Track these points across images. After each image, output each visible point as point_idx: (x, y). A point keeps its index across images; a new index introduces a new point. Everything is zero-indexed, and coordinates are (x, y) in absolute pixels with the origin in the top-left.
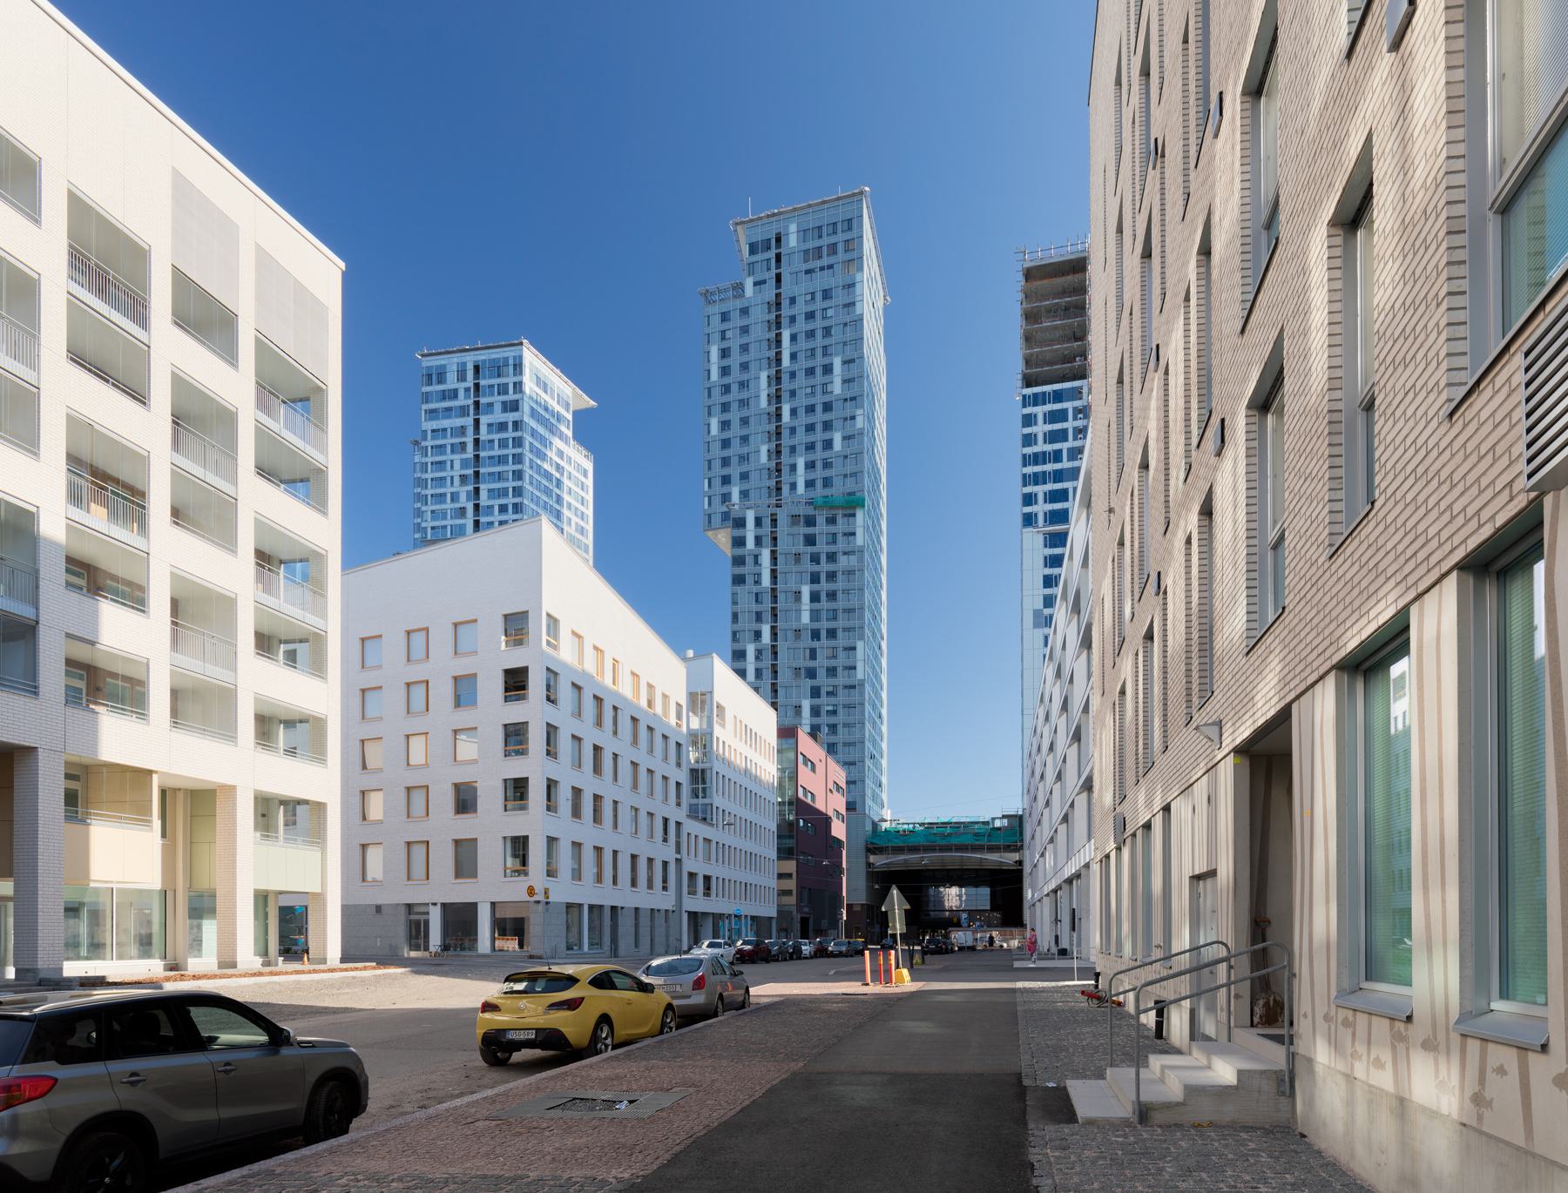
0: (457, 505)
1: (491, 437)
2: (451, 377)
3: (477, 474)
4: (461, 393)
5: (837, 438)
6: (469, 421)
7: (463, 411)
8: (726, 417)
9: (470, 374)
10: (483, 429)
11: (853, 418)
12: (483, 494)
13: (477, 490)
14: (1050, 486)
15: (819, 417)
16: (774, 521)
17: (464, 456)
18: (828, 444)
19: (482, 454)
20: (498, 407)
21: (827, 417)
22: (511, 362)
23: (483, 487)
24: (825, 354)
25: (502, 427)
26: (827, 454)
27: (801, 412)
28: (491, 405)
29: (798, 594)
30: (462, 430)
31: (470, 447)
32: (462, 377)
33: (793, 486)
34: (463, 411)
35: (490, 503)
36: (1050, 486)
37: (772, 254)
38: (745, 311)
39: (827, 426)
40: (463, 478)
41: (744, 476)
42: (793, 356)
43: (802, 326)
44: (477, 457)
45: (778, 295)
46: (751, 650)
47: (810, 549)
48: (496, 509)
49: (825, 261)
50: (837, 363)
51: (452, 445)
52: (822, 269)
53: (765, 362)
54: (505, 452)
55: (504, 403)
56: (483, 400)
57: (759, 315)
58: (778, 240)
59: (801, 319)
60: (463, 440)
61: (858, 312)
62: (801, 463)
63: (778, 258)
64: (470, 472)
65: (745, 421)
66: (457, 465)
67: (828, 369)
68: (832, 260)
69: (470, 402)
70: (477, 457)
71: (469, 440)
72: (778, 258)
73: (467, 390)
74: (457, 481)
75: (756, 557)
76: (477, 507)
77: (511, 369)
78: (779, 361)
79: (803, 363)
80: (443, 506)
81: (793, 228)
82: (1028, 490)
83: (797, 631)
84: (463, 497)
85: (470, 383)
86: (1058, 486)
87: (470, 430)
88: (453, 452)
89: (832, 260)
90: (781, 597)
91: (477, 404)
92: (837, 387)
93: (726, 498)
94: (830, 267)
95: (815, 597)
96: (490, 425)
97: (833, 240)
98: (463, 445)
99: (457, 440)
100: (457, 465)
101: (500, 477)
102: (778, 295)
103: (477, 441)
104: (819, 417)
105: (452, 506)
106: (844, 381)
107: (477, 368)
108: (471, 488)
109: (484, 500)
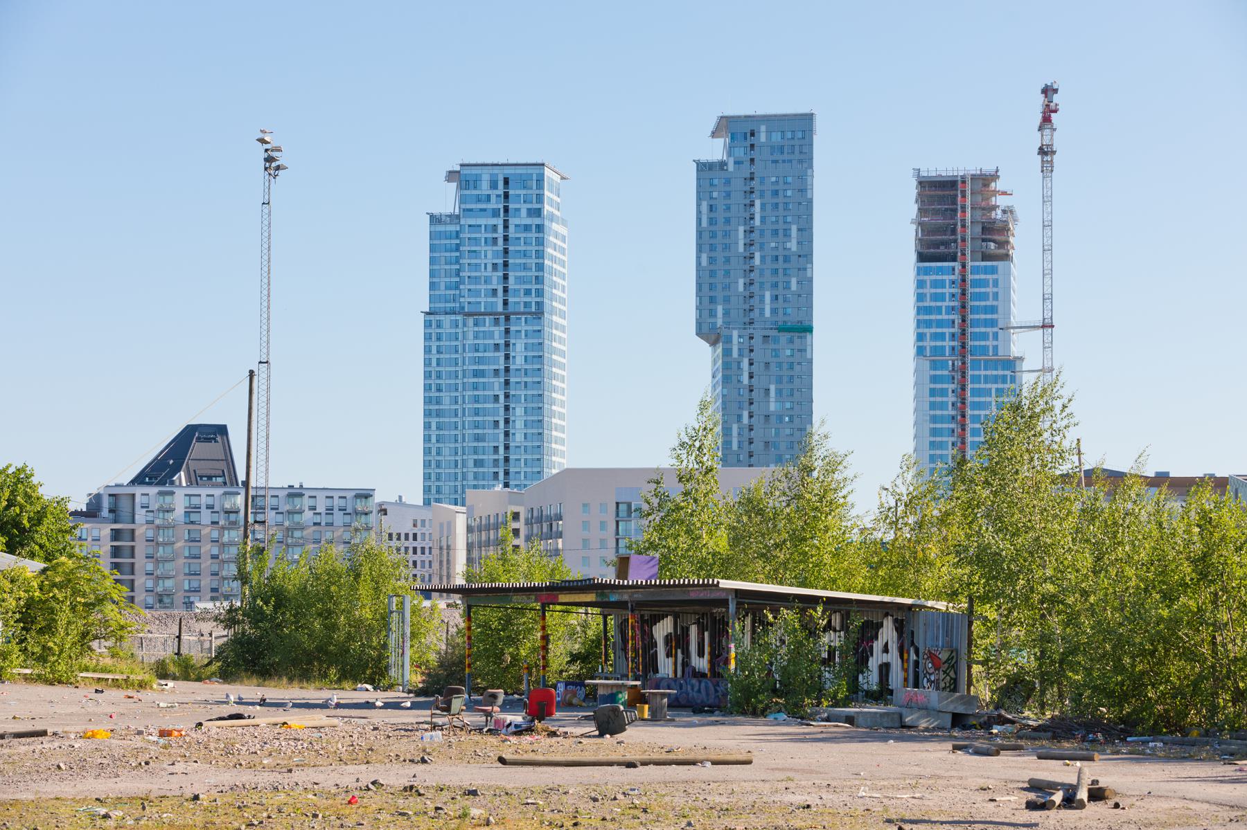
0: (490, 287)
1: (518, 235)
2: (485, 185)
3: (506, 264)
6: (499, 222)
7: (495, 213)
8: (713, 254)
9: (501, 184)
10: (512, 228)
11: (805, 269)
12: (511, 280)
13: (506, 277)
17: (495, 248)
18: (787, 286)
20: (524, 213)
22: (535, 177)
23: (511, 275)
25: (527, 228)
27: (768, 259)
28: (518, 210)
29: (768, 390)
31: (501, 241)
32: (494, 185)
33: (762, 310)
35: (517, 287)
38: (728, 182)
40: (495, 266)
41: (727, 300)
42: (763, 219)
43: (768, 198)
44: (506, 251)
46: (735, 427)
47: (775, 360)
48: (522, 292)
49: (786, 157)
50: (794, 228)
52: (784, 161)
53: (742, 220)
54: (529, 248)
55: (529, 210)
56: (511, 206)
57: (738, 185)
58: (752, 134)
59: (768, 194)
64: (500, 261)
65: (728, 260)
66: (490, 255)
67: (787, 233)
68: (790, 157)
69: (501, 206)
70: (506, 251)
73: (498, 196)
74: (490, 267)
75: (739, 363)
76: (506, 290)
77: (535, 182)
80: (478, 287)
81: (763, 128)
83: (767, 417)
84: (495, 280)
87: (501, 228)
89: (790, 157)
91: (506, 210)
92: (793, 245)
93: (712, 314)
94: (790, 161)
95: (779, 392)
97: (792, 143)
99: (490, 235)
100: (490, 255)
101: (525, 267)
103: (506, 239)
105: (485, 287)
107: (506, 181)
108: (501, 274)
109: (512, 284)
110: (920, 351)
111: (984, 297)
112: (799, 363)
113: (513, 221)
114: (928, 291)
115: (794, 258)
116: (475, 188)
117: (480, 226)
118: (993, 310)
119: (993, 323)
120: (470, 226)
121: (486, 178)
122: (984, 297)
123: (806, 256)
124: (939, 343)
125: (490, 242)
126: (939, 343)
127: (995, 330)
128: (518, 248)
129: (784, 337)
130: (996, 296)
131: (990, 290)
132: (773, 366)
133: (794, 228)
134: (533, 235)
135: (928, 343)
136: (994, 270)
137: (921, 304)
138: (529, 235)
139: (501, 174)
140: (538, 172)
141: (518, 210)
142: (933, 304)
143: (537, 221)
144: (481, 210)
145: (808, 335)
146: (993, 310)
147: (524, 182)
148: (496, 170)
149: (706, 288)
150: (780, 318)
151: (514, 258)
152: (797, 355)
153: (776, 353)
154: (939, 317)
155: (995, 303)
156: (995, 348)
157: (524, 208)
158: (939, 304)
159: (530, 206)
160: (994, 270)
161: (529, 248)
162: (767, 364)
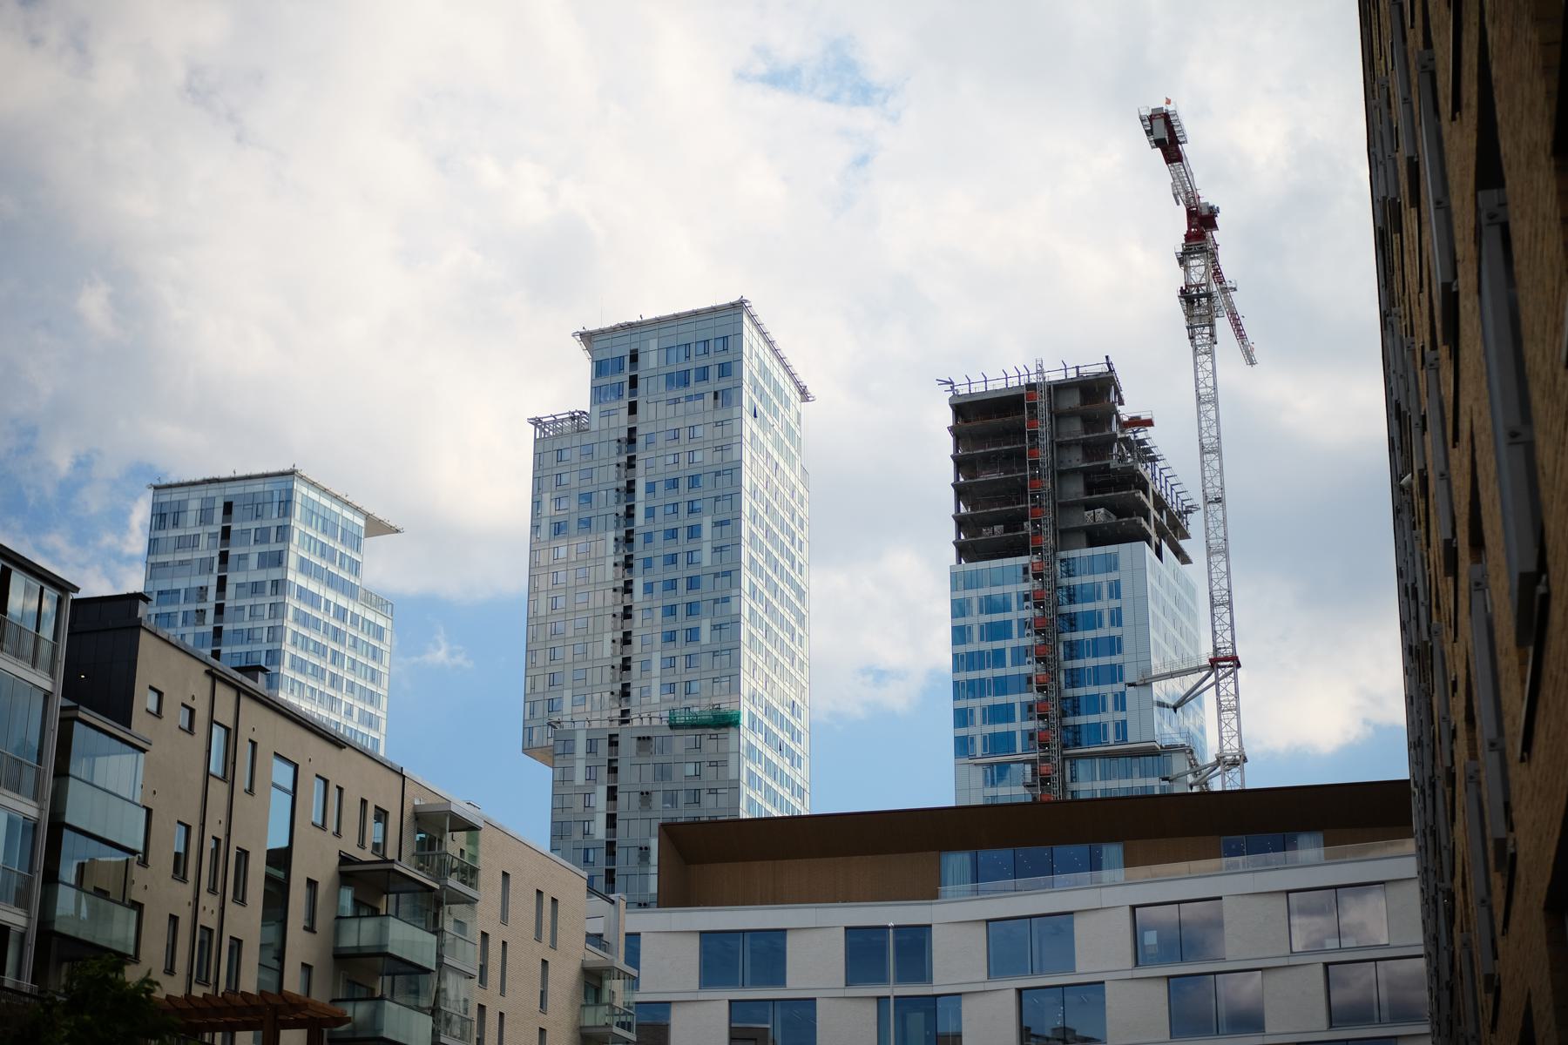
1: (240, 603)
2: (192, 516)
4: (204, 541)
5: (705, 626)
6: (213, 582)
9: (218, 514)
10: (230, 590)
11: (726, 600)
14: (989, 700)
15: (682, 596)
16: (613, 742)
18: (693, 635)
19: (227, 627)
20: (253, 560)
21: (693, 597)
24: (691, 511)
25: (256, 588)
26: (692, 649)
28: (243, 557)
30: (203, 591)
31: (210, 616)
32: (205, 517)
34: (205, 565)
36: (989, 700)
37: (624, 377)
39: (692, 609)
42: (650, 513)
44: (218, 632)
45: (632, 431)
50: (707, 523)
51: (185, 613)
56: (233, 551)
58: (634, 358)
60: (201, 606)
61: (736, 457)
62: (656, 659)
63: (633, 382)
67: (694, 532)
69: (215, 554)
70: (218, 632)
71: (210, 606)
72: (633, 382)
78: (630, 514)
79: (662, 523)
81: (653, 344)
82: (962, 704)
85: (217, 528)
86: (1001, 700)
88: (185, 622)
90: (620, 854)
91: (224, 557)
96: (238, 586)
98: (201, 613)
99: (192, 607)
102: (632, 431)
103: (220, 609)
104: (682, 596)
106: (715, 549)
107: (228, 508)
110: (963, 746)
111: (1093, 620)
112: (713, 791)
113: (233, 578)
114: (976, 620)
115: (706, 582)
116: (176, 525)
117: (178, 591)
118: (1114, 645)
119: (1115, 674)
120: (160, 593)
121: (194, 505)
122: (1093, 620)
123: (728, 573)
124: (1001, 728)
125: (192, 618)
126: (1001, 728)
127: (1119, 687)
128: (238, 626)
129: (681, 742)
130: (1116, 617)
131: (1104, 605)
132: (657, 799)
133: (707, 523)
134: (267, 600)
135: (980, 730)
136: (1111, 564)
137: (962, 649)
138: (259, 601)
139: (219, 495)
140: (282, 486)
141: (243, 557)
142: (987, 646)
143: (275, 574)
144: (182, 563)
145: (732, 730)
146: (1114, 645)
147: (257, 507)
148: (213, 491)
149: (542, 658)
150: (680, 702)
151: (235, 643)
152: (710, 773)
153: (663, 772)
154: (999, 672)
155: (1115, 631)
156: (1122, 728)
157: (254, 552)
158: (998, 645)
159: (264, 548)
160: (1111, 564)
161: (257, 624)
162: (646, 795)
